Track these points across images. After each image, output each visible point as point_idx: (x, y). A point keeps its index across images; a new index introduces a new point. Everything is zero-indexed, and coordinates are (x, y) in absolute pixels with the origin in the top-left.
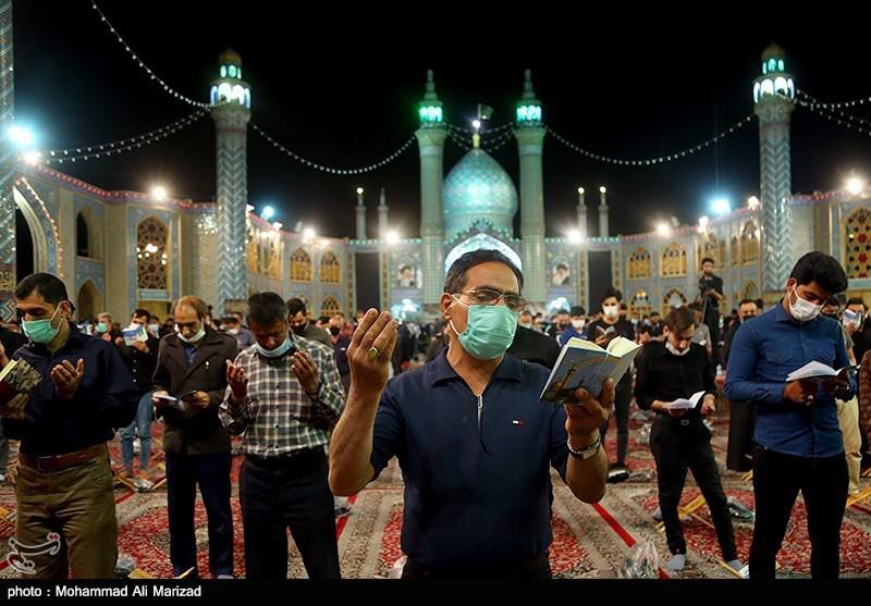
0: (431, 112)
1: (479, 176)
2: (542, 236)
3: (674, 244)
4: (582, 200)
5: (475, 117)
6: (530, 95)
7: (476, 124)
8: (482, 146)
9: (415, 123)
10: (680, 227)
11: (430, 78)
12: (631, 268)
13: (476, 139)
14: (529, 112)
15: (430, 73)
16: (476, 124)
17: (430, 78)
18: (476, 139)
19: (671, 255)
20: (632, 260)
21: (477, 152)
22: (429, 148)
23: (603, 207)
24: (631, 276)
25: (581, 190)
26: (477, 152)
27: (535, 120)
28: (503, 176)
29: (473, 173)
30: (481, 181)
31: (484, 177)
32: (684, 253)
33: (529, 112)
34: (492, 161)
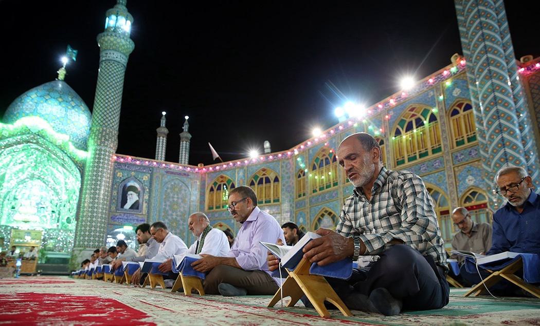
1: (56, 99)
2: (114, 152)
3: (264, 170)
4: (163, 122)
7: (65, 60)
8: (67, 79)
10: (272, 152)
13: (62, 73)
18: (62, 73)
19: (261, 182)
20: (212, 190)
24: (210, 208)
25: (164, 113)
27: (125, 32)
28: (83, 107)
29: (48, 95)
30: (57, 103)
31: (60, 100)
32: (276, 180)
34: (73, 91)
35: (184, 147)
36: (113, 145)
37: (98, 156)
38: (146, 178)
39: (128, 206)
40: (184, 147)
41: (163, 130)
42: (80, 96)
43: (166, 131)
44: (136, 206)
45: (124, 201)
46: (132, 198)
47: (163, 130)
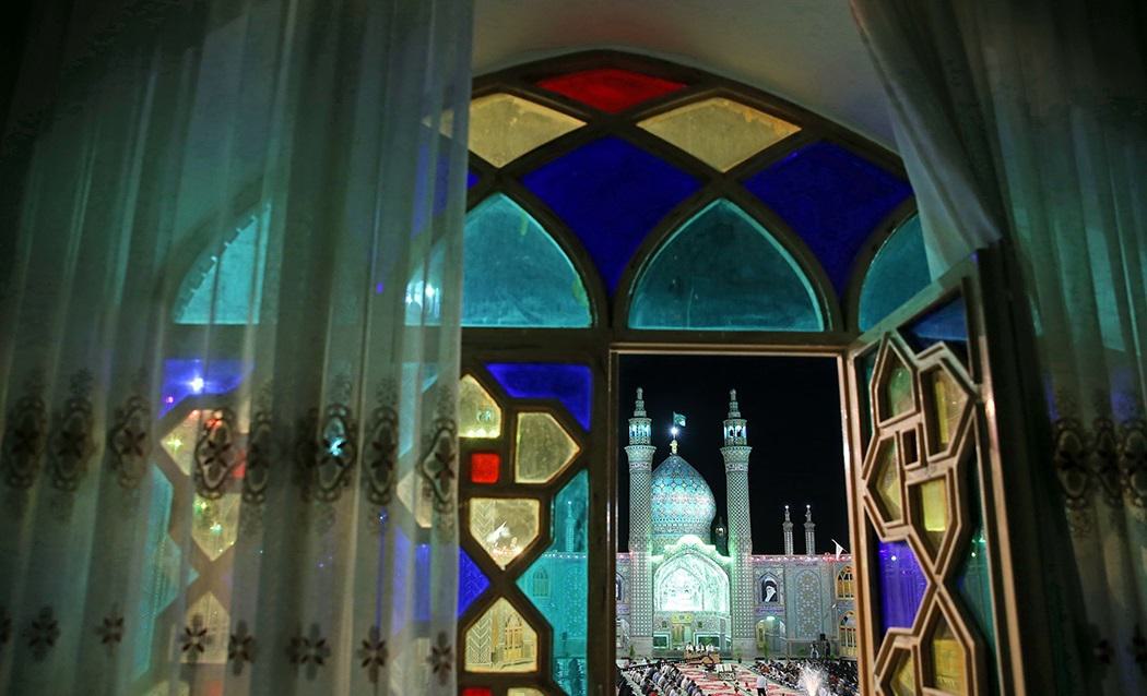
0: (640, 428)
5: (670, 421)
6: (738, 414)
7: (674, 431)
8: (680, 452)
9: (625, 439)
11: (640, 396)
12: (840, 589)
13: (674, 445)
14: (736, 428)
15: (640, 391)
16: (674, 431)
17: (640, 396)
18: (674, 445)
20: (840, 578)
21: (674, 460)
22: (639, 455)
23: (809, 525)
26: (674, 460)
33: (736, 428)
35: (810, 538)
36: (749, 547)
37: (740, 560)
38: (780, 572)
39: (767, 600)
40: (810, 538)
41: (788, 525)
42: (705, 479)
43: (791, 525)
44: (774, 598)
45: (765, 596)
46: (771, 592)
47: (788, 525)
